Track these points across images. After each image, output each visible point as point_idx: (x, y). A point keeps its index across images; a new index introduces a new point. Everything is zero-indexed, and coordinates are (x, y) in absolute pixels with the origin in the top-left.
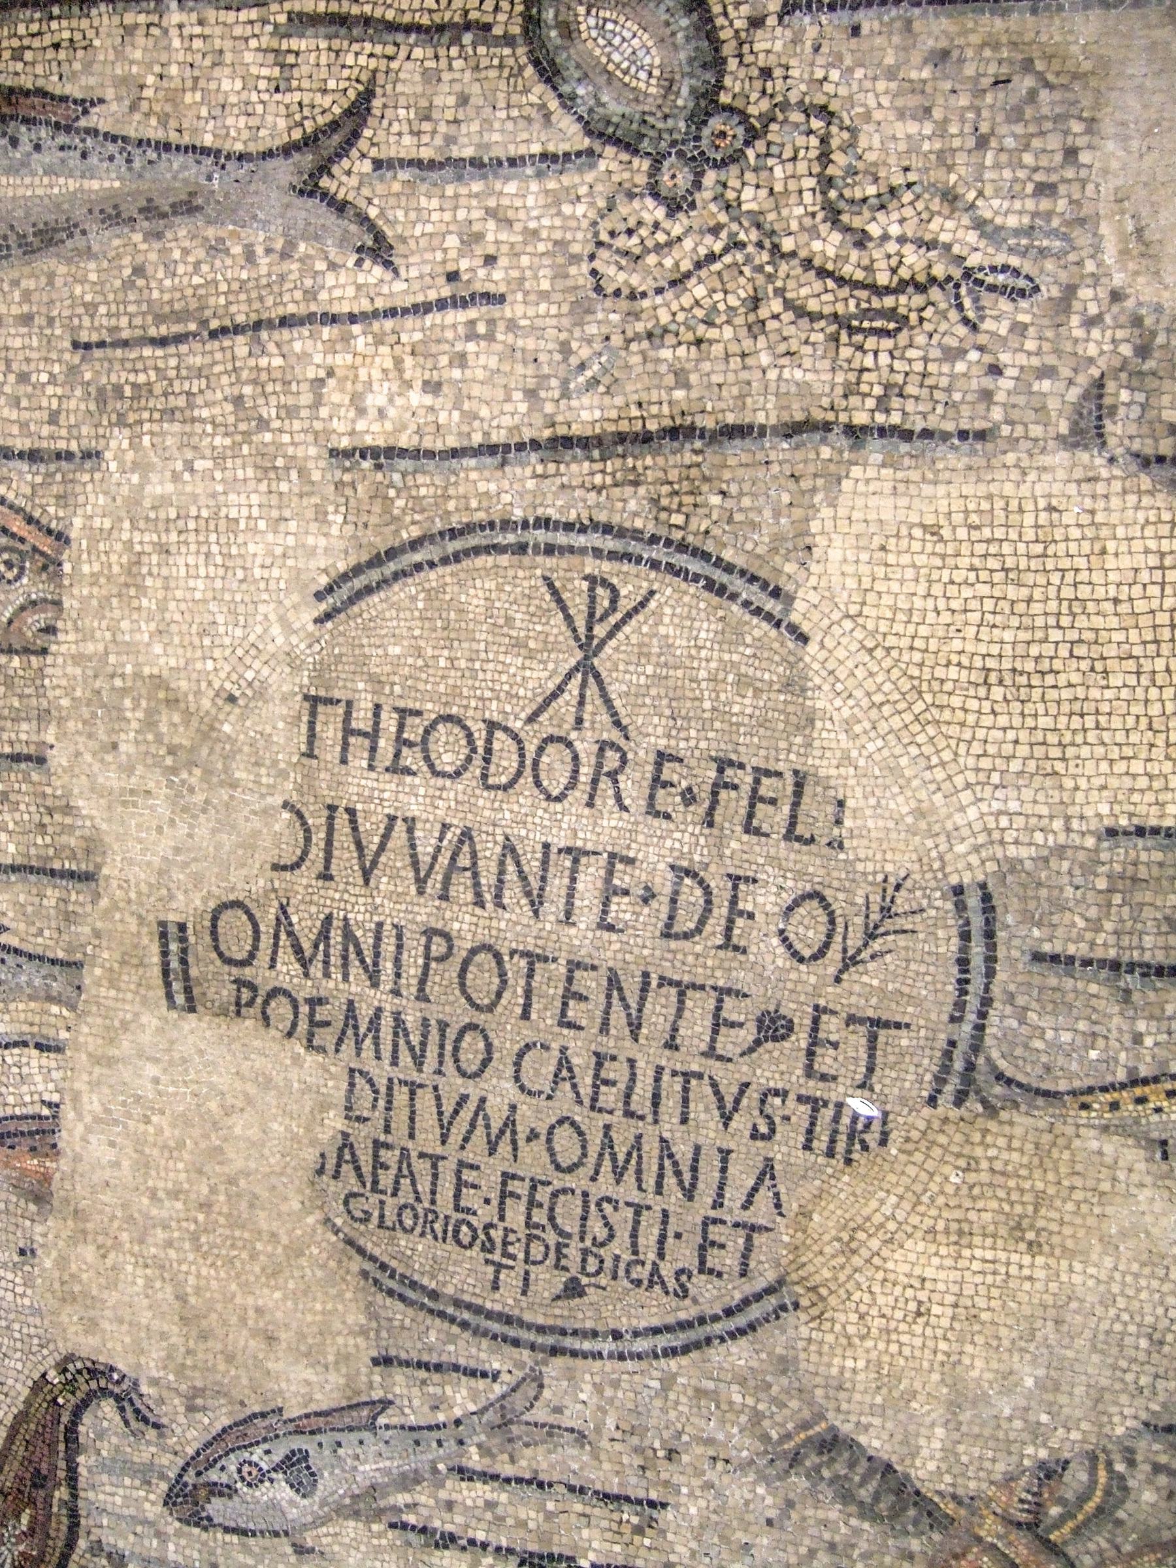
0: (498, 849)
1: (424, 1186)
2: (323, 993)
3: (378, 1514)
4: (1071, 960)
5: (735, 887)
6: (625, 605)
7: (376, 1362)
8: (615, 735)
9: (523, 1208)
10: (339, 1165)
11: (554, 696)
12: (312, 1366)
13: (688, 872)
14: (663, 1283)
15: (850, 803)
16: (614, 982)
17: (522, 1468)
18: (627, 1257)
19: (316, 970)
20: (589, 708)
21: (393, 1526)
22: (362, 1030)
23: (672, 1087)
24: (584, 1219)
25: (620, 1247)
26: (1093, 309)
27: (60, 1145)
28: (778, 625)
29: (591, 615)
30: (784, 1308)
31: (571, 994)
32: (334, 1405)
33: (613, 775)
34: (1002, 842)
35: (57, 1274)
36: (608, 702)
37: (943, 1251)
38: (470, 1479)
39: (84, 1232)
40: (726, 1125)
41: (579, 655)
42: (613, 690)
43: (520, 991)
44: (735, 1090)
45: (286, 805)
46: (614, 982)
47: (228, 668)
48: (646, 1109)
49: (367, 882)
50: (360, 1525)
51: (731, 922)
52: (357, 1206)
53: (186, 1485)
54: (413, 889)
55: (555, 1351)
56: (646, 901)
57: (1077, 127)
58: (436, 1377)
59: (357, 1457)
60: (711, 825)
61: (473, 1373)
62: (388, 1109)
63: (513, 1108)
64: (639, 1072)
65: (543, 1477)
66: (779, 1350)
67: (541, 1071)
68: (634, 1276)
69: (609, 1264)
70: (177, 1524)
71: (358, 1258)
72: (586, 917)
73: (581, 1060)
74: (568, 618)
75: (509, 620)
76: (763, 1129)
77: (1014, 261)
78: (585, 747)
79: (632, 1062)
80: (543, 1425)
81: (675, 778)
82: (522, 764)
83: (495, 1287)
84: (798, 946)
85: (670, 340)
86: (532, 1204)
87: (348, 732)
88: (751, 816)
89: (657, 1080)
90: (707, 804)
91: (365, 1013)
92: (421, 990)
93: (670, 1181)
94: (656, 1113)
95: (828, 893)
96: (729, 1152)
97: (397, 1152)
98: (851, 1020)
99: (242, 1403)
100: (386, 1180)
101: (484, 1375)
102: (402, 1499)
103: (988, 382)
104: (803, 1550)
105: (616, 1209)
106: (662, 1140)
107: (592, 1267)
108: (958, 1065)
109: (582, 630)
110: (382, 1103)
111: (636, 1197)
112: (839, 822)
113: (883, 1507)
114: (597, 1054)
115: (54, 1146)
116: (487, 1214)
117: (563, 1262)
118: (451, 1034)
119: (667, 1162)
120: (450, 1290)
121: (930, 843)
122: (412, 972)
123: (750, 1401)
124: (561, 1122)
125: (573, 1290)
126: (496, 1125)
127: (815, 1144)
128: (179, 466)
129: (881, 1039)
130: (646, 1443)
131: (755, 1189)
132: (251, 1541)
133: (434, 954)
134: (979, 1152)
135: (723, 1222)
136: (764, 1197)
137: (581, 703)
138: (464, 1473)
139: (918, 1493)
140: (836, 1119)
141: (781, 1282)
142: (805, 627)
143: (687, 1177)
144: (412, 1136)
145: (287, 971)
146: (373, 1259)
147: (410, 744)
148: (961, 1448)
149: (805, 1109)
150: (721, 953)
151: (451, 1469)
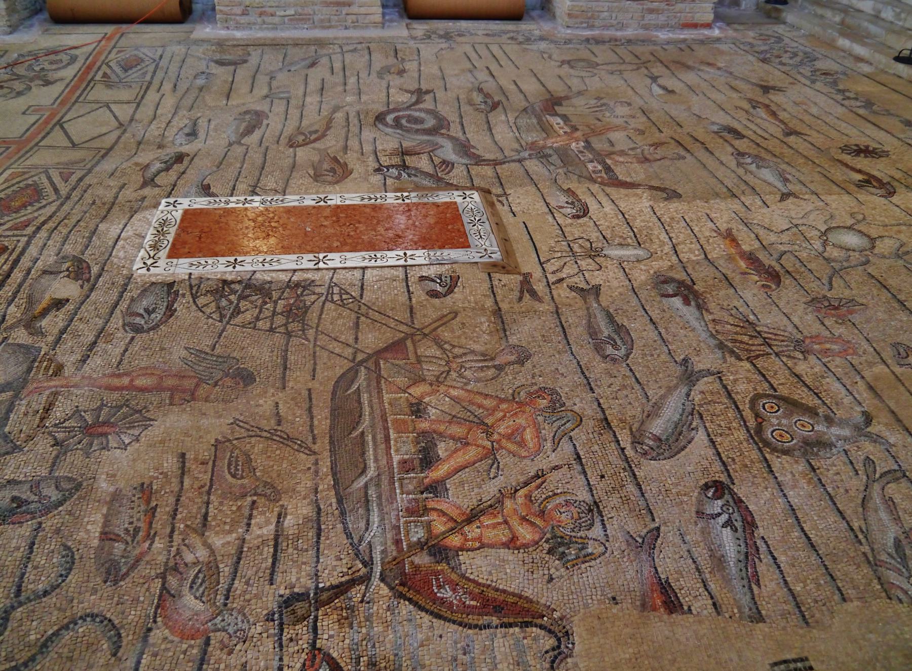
35: (610, 615)
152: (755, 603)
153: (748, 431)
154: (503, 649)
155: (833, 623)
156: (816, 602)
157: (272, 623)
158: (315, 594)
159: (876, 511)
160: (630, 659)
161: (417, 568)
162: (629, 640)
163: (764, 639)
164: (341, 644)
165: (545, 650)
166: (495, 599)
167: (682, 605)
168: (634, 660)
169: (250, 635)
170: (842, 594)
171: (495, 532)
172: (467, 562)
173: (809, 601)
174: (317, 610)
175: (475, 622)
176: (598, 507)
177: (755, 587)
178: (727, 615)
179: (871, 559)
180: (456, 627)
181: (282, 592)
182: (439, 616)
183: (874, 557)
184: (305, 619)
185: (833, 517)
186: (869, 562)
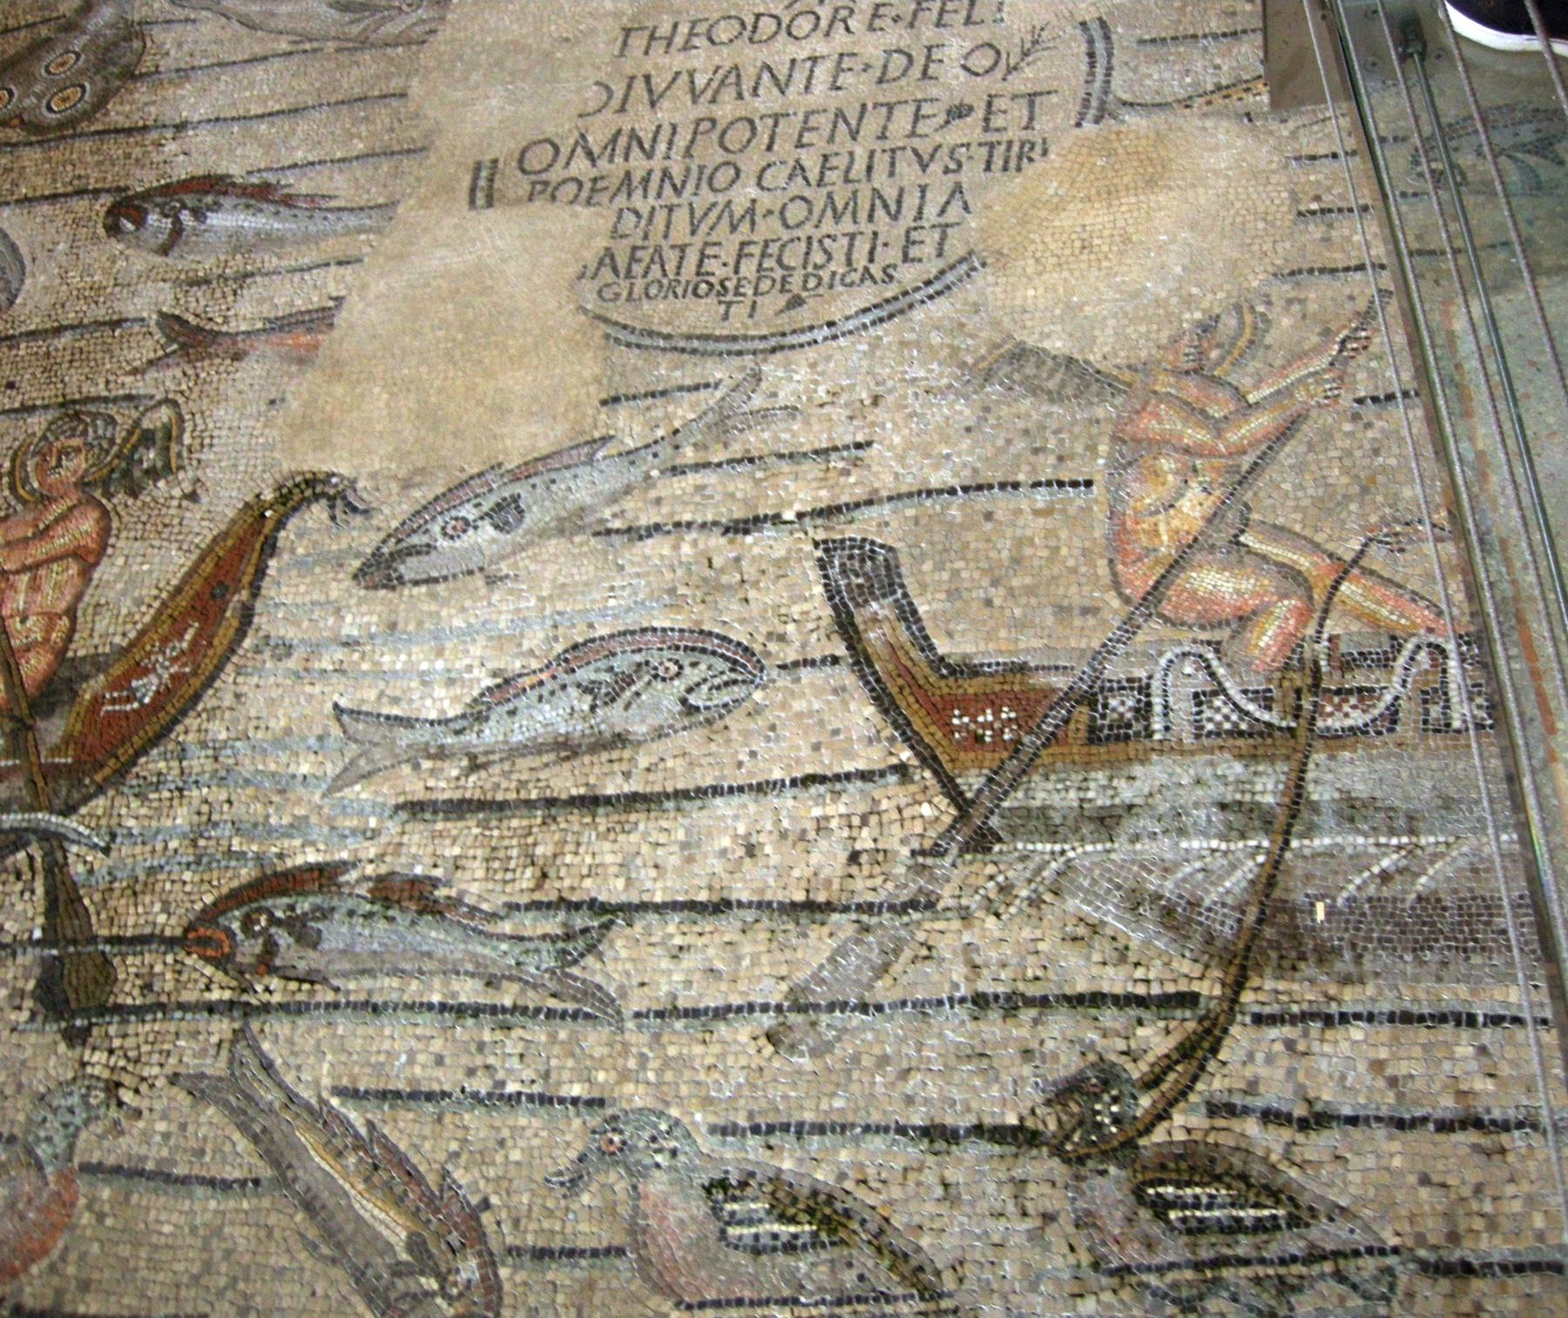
1: (670, 267)
3: (581, 529)
4: (1164, 40)
7: (604, 403)
17: (736, 450)
18: (841, 271)
30: (974, 269)
52: (607, 294)
55: (773, 350)
58: (659, 401)
65: (755, 453)
69: (826, 279)
70: (362, 593)
76: (952, 166)
79: (851, 154)
86: (763, 255)
87: (652, 37)
91: (637, 177)
98: (1014, 97)
99: (462, 470)
100: (638, 269)
101: (707, 386)
102: (607, 513)
104: (1000, 442)
107: (812, 283)
111: (851, 228)
113: (1069, 391)
116: (720, 272)
118: (707, 172)
120: (684, 329)
123: (948, 341)
125: (796, 302)
130: (855, 396)
132: (441, 588)
138: (676, 470)
143: (893, 208)
146: (616, 324)
148: (1129, 330)
149: (984, 151)
151: (662, 472)
153: (31, 144)
154: (302, 589)
156: (392, 130)
157: (95, 1031)
158: (54, 945)
159: (273, 15)
160: (392, 394)
161: (68, 739)
164: (188, 888)
166: (197, 594)
167: (324, 309)
169: (106, 1074)
171: (47, 588)
172: (96, 641)
174: (94, 939)
175: (231, 632)
176: (74, 402)
177: (333, 204)
180: (229, 668)
181: (25, 1015)
182: (197, 697)
184: (107, 962)
185: (259, 72)
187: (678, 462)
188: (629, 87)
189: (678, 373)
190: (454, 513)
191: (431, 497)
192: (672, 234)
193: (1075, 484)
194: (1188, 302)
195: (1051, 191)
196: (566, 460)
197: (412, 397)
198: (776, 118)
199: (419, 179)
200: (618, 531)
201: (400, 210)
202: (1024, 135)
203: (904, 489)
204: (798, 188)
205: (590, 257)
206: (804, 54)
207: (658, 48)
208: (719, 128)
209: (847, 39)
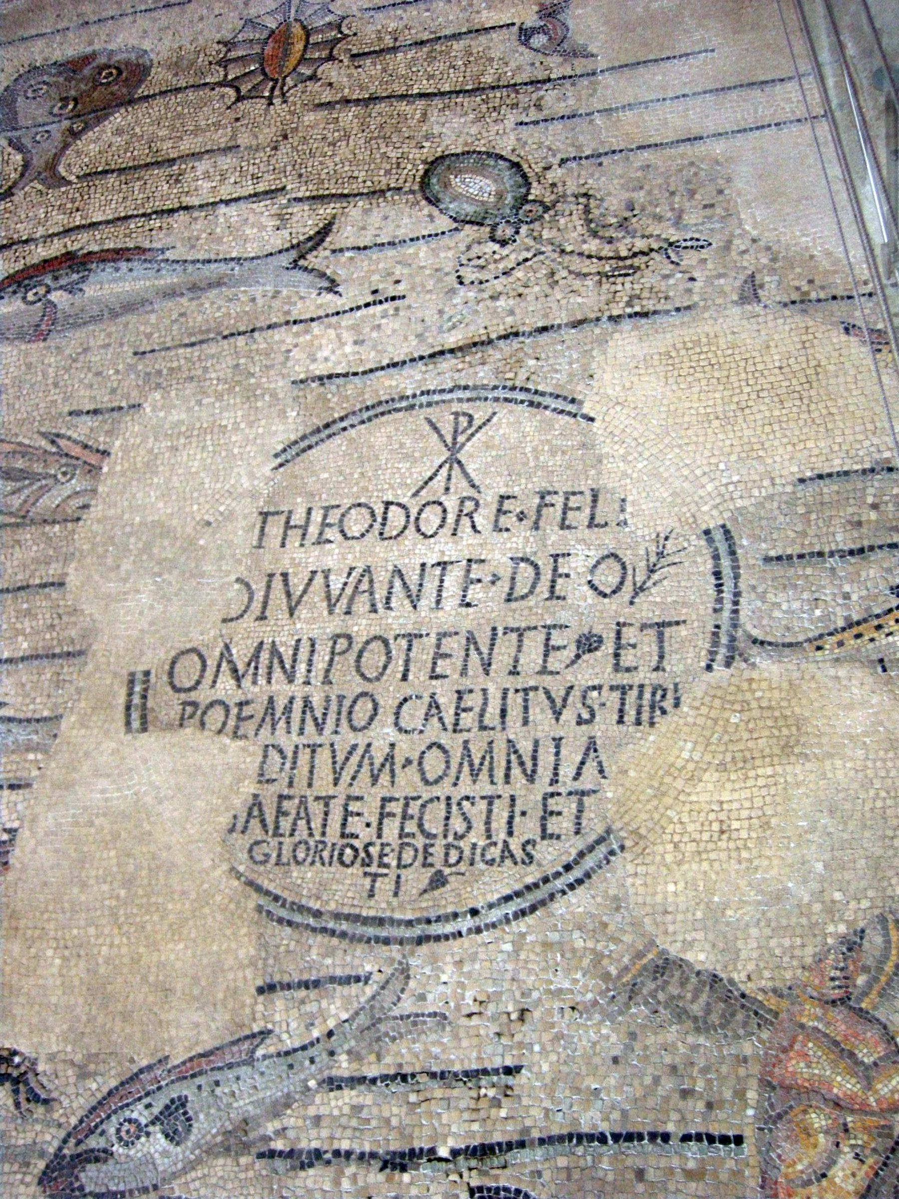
0: (389, 575)
1: (316, 824)
2: (249, 696)
3: (246, 1147)
4: (790, 557)
5: (556, 561)
6: (477, 423)
7: (261, 991)
8: (472, 492)
9: (398, 820)
10: (247, 822)
11: (431, 479)
12: (202, 1008)
13: (522, 560)
14: (512, 856)
15: (630, 498)
16: (471, 639)
18: (482, 843)
19: (246, 683)
20: (453, 480)
21: (261, 1156)
22: (278, 715)
23: (515, 702)
24: (447, 818)
25: (477, 837)
26: (743, 248)
27: (11, 862)
28: (575, 416)
29: (456, 431)
30: (612, 853)
31: (439, 655)
32: (217, 1043)
33: (470, 515)
34: (732, 499)
36: (466, 475)
37: (733, 777)
38: (339, 1088)
39: (17, 929)
40: (557, 719)
41: (447, 454)
42: (470, 469)
43: (401, 662)
44: (562, 693)
45: (238, 580)
46: (471, 639)
47: (207, 506)
48: (497, 722)
49: (291, 615)
50: (229, 1161)
51: (553, 581)
53: (64, 1156)
54: (325, 613)
55: (421, 941)
56: (493, 583)
57: (721, 182)
58: (313, 994)
59: (233, 1094)
60: (537, 528)
61: (347, 980)
62: (292, 769)
63: (392, 745)
64: (490, 696)
65: (407, 1070)
66: (612, 892)
67: (413, 715)
68: (488, 857)
69: (467, 853)
71: (255, 895)
72: (450, 602)
73: (446, 700)
74: (441, 436)
75: (402, 445)
76: (586, 716)
77: (696, 236)
78: (451, 503)
79: (484, 691)
80: (409, 1016)
81: (511, 508)
82: (408, 521)
83: (371, 895)
84: (601, 588)
85: (503, 298)
86: (405, 817)
87: (288, 526)
88: (564, 519)
89: (504, 698)
90: (534, 518)
91: (281, 703)
92: (326, 677)
93: (516, 771)
94: (503, 723)
95: (619, 552)
96: (561, 739)
97: (297, 801)
98: (643, 627)
99: (132, 1061)
100: (285, 824)
101: (358, 979)
102: (270, 1127)
103: (690, 285)
104: (648, 1080)
105: (473, 804)
106: (509, 741)
107: (453, 857)
108: (724, 640)
109: (449, 440)
110: (288, 765)
111: (488, 790)
112: (623, 510)
113: (714, 1018)
114: (458, 692)
115: (6, 863)
116: (366, 835)
117: (430, 860)
118: (347, 703)
119: (513, 757)
120: (332, 906)
121: (684, 509)
122: (320, 665)
123: (590, 944)
124: (430, 747)
125: (438, 881)
126: (378, 762)
127: (626, 719)
128: (193, 403)
129: (667, 635)
130: (502, 1008)
131: (583, 763)
133: (337, 650)
134: (748, 696)
135: (559, 794)
136: (590, 768)
137: (449, 478)
138: (333, 1084)
139: (743, 996)
140: (640, 696)
141: (608, 831)
142: (592, 415)
143: (529, 765)
144: (310, 785)
145: (226, 687)
146: (268, 893)
147: (329, 525)
148: (773, 943)
149: (616, 695)
150: (548, 603)
151: (320, 1084)
152: (29, 721)
155: (91, 615)
160: (64, 959)
162: (33, 950)
163: (87, 727)
165: (12, 1108)
168: (67, 953)
170: (53, 584)
173: (48, 636)
178: (35, 773)
179: (13, 520)
183: (11, 514)
186: (17, 525)
187: (334, 1073)
188: (269, 587)
189: (329, 961)
190: (127, 1113)
191: (105, 1090)
192: (316, 783)
193: (725, 1140)
194: (832, 910)
195: (685, 755)
196: (229, 1059)
197: (82, 964)
198: (411, 638)
199: (79, 691)
200: (281, 1153)
201: (64, 725)
202: (655, 678)
203: (555, 1131)
204: (433, 731)
205: (240, 803)
206: (432, 559)
207: (294, 537)
208: (356, 647)
209: (475, 540)
